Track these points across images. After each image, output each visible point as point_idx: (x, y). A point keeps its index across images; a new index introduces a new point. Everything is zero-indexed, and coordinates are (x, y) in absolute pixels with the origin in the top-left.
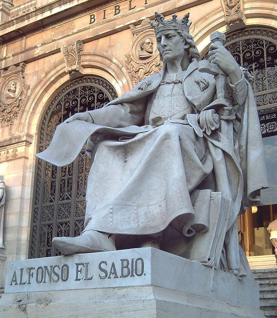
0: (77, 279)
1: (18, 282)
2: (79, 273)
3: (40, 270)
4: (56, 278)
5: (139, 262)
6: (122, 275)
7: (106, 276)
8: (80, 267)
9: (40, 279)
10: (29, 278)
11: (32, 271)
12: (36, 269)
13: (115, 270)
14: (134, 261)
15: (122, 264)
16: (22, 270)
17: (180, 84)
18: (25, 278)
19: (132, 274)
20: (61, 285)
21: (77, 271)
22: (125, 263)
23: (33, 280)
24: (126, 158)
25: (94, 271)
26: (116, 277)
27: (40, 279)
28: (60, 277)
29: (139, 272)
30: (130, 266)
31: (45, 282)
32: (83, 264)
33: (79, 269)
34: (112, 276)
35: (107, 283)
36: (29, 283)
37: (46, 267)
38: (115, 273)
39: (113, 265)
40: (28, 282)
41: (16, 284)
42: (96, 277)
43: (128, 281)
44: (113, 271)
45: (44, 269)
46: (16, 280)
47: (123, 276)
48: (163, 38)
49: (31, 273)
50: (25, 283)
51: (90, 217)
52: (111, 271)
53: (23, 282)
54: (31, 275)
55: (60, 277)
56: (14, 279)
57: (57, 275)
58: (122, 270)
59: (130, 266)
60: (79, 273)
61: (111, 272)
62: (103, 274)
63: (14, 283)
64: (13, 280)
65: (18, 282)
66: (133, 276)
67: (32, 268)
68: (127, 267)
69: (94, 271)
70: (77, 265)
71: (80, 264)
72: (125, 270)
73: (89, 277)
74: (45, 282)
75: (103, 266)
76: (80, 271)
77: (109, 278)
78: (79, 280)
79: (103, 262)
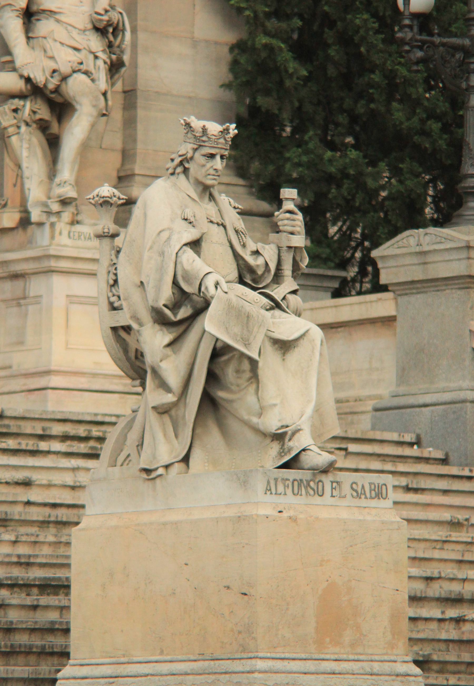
0: (332, 496)
1: (274, 491)
2: (334, 490)
3: (296, 483)
4: (312, 492)
5: (384, 487)
6: (371, 497)
7: (358, 496)
8: (335, 485)
9: (296, 491)
10: (285, 489)
11: (287, 482)
12: (291, 480)
13: (365, 491)
14: (380, 485)
15: (370, 487)
16: (276, 480)
17: (221, 228)
18: (281, 488)
19: (379, 497)
20: (317, 500)
21: (332, 488)
22: (373, 487)
23: (289, 491)
24: (284, 356)
25: (346, 489)
26: (366, 498)
27: (296, 491)
28: (316, 492)
29: (384, 495)
30: (377, 490)
31: (301, 495)
32: (337, 482)
33: (334, 487)
34: (363, 497)
35: (357, 502)
36: (285, 494)
37: (301, 480)
38: (365, 494)
39: (363, 487)
40: (283, 493)
41: (271, 493)
42: (349, 496)
43: (374, 503)
44: (363, 492)
45: (299, 481)
46: (270, 490)
47: (371, 498)
48: (218, 158)
49: (287, 484)
50: (281, 494)
51: (299, 428)
52: (361, 492)
53: (279, 492)
54: (286, 487)
55: (316, 492)
56: (269, 488)
57: (313, 490)
58: (370, 492)
59: (377, 490)
60: (334, 490)
61: (361, 493)
62: (355, 494)
63: (268, 493)
64: (267, 489)
65: (274, 491)
66: (379, 498)
67: (287, 480)
68: (375, 490)
69: (346, 489)
70: (332, 482)
71: (334, 482)
72: (373, 493)
73: (343, 495)
74: (301, 495)
75: (354, 486)
76: (335, 489)
77: (360, 498)
78: (334, 497)
79: (355, 483)
